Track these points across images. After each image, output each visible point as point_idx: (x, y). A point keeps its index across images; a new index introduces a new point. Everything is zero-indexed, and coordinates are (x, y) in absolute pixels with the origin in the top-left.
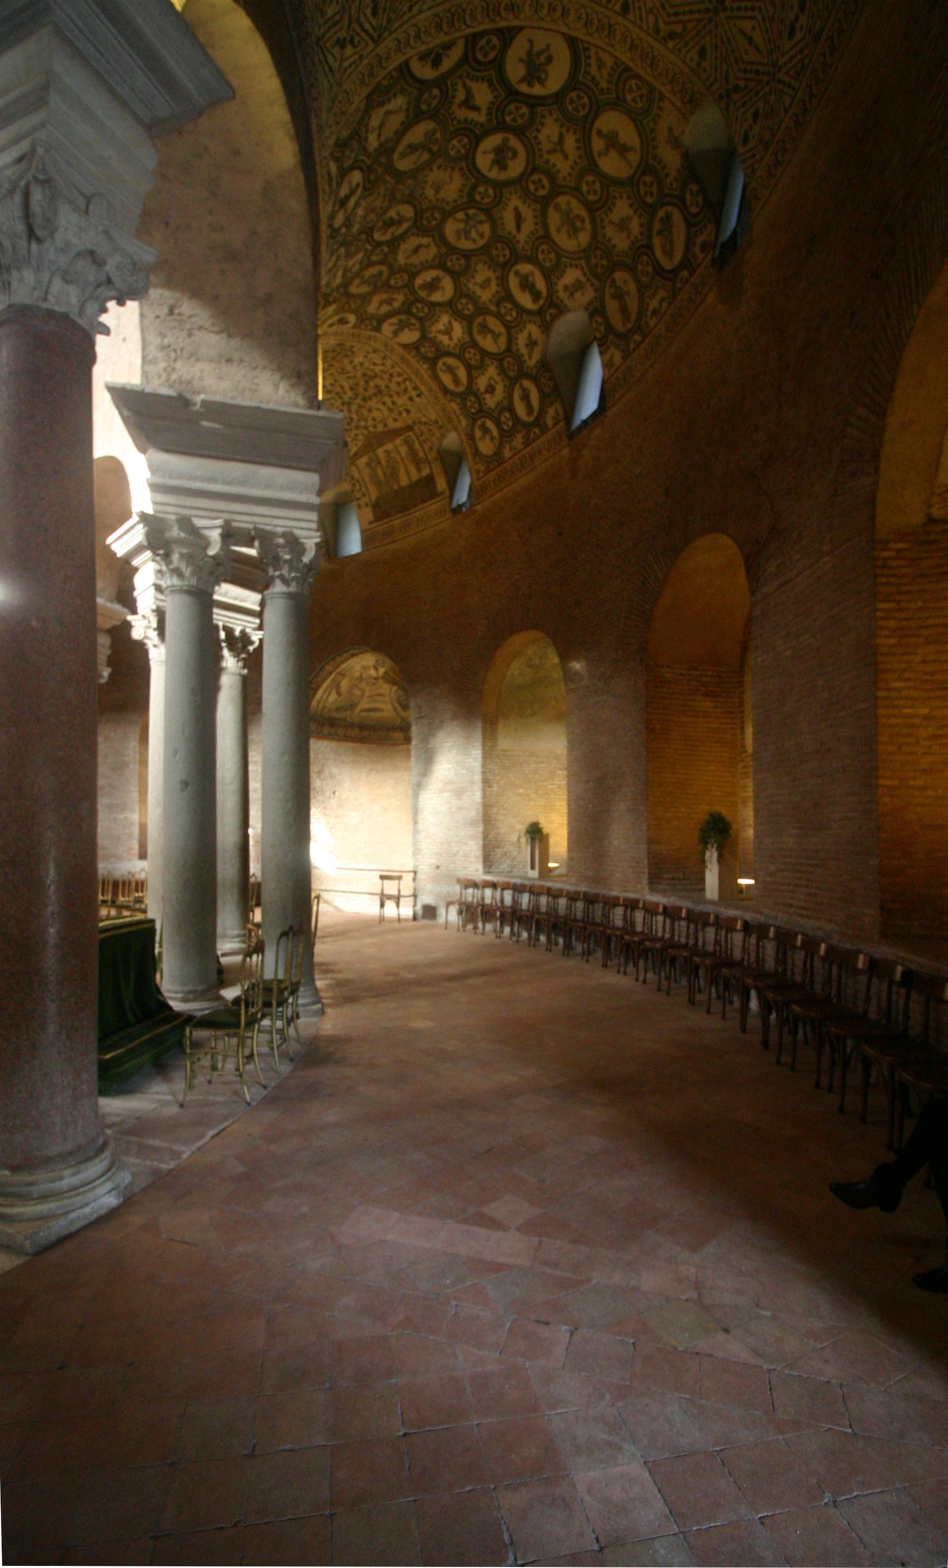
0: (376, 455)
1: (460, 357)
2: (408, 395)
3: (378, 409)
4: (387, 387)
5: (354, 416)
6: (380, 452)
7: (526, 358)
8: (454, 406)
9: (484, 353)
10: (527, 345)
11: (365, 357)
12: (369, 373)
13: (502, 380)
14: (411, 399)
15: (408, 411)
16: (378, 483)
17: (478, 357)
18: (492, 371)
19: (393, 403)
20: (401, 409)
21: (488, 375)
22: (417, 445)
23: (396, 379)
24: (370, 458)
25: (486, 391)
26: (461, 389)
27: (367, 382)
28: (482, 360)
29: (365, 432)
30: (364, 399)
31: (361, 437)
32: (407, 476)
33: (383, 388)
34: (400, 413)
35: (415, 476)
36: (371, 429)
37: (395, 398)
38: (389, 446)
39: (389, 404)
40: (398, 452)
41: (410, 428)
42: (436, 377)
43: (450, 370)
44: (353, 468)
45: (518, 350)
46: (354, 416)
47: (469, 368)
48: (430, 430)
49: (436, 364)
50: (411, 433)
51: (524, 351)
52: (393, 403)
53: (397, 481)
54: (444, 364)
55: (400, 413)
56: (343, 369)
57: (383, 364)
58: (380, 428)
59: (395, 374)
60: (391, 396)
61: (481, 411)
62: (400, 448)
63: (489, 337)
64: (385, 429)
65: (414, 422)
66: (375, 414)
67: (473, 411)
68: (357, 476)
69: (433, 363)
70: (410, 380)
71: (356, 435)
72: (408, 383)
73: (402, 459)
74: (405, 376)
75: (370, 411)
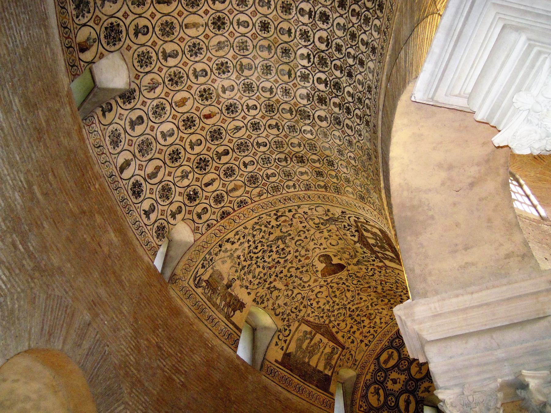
0: (315, 335)
1: (400, 358)
2: (363, 339)
3: (346, 324)
4: (364, 326)
5: (336, 313)
6: (318, 337)
7: (420, 391)
8: (373, 367)
9: (409, 369)
10: (425, 388)
11: (387, 315)
12: (373, 317)
13: (403, 385)
14: (362, 341)
15: (353, 342)
16: (299, 347)
17: (405, 367)
18: (403, 377)
19: (354, 332)
20: (352, 338)
21: (400, 376)
22: (337, 356)
23: (372, 331)
24: (311, 332)
25: (392, 380)
26: (384, 366)
27: (365, 316)
28: (405, 370)
29: (327, 322)
30: (350, 315)
31: (322, 320)
32: (317, 362)
33: (362, 324)
34: (349, 338)
35: (321, 367)
36: (331, 325)
37: (357, 333)
38: (325, 340)
39: (352, 330)
40: (325, 347)
41: (343, 348)
42: (383, 350)
43: (390, 356)
44: (297, 324)
45: (420, 385)
46: (336, 313)
47: (396, 366)
48: (349, 359)
49: (390, 348)
50: (340, 349)
51: (422, 389)
52: (354, 332)
53: (310, 358)
54: (392, 352)
55: (349, 338)
56: (376, 305)
57: (381, 323)
58: (334, 330)
59: (375, 329)
60: (358, 329)
61: (382, 383)
62: (328, 347)
63: (418, 368)
64: (335, 334)
65: (348, 348)
66: (343, 325)
67: (378, 378)
68: (293, 328)
69: (391, 346)
70: (374, 337)
71: (322, 317)
72: (372, 337)
73: (323, 352)
74: (376, 335)
75: (343, 321)
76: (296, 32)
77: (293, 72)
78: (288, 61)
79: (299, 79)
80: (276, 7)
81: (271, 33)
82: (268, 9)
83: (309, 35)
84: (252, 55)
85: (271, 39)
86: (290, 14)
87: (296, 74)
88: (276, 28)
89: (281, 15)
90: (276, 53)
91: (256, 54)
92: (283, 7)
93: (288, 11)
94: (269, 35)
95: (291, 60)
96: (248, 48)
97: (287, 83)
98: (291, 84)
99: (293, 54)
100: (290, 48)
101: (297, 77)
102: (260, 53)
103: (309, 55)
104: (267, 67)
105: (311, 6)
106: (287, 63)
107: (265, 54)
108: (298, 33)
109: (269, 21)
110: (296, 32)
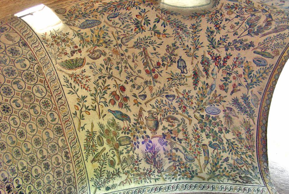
76: (30, 153)
77: (11, 163)
78: (14, 157)
79: (10, 168)
80: (34, 135)
81: (21, 139)
82: (30, 132)
83: (34, 162)
84: (4, 134)
85: (18, 141)
86: (36, 145)
87: (12, 165)
88: (25, 141)
89: (33, 141)
90: (14, 147)
91: (5, 137)
92: (37, 140)
93: (37, 143)
94: (19, 138)
95: (16, 158)
96: (6, 130)
97: (3, 162)
98: (5, 165)
99: (20, 158)
100: (21, 154)
101: (11, 167)
102: (7, 138)
103: (24, 168)
104: (4, 146)
105: (47, 155)
106: (13, 157)
107: (9, 142)
108: (30, 155)
109: (26, 135)
110: (30, 153)
